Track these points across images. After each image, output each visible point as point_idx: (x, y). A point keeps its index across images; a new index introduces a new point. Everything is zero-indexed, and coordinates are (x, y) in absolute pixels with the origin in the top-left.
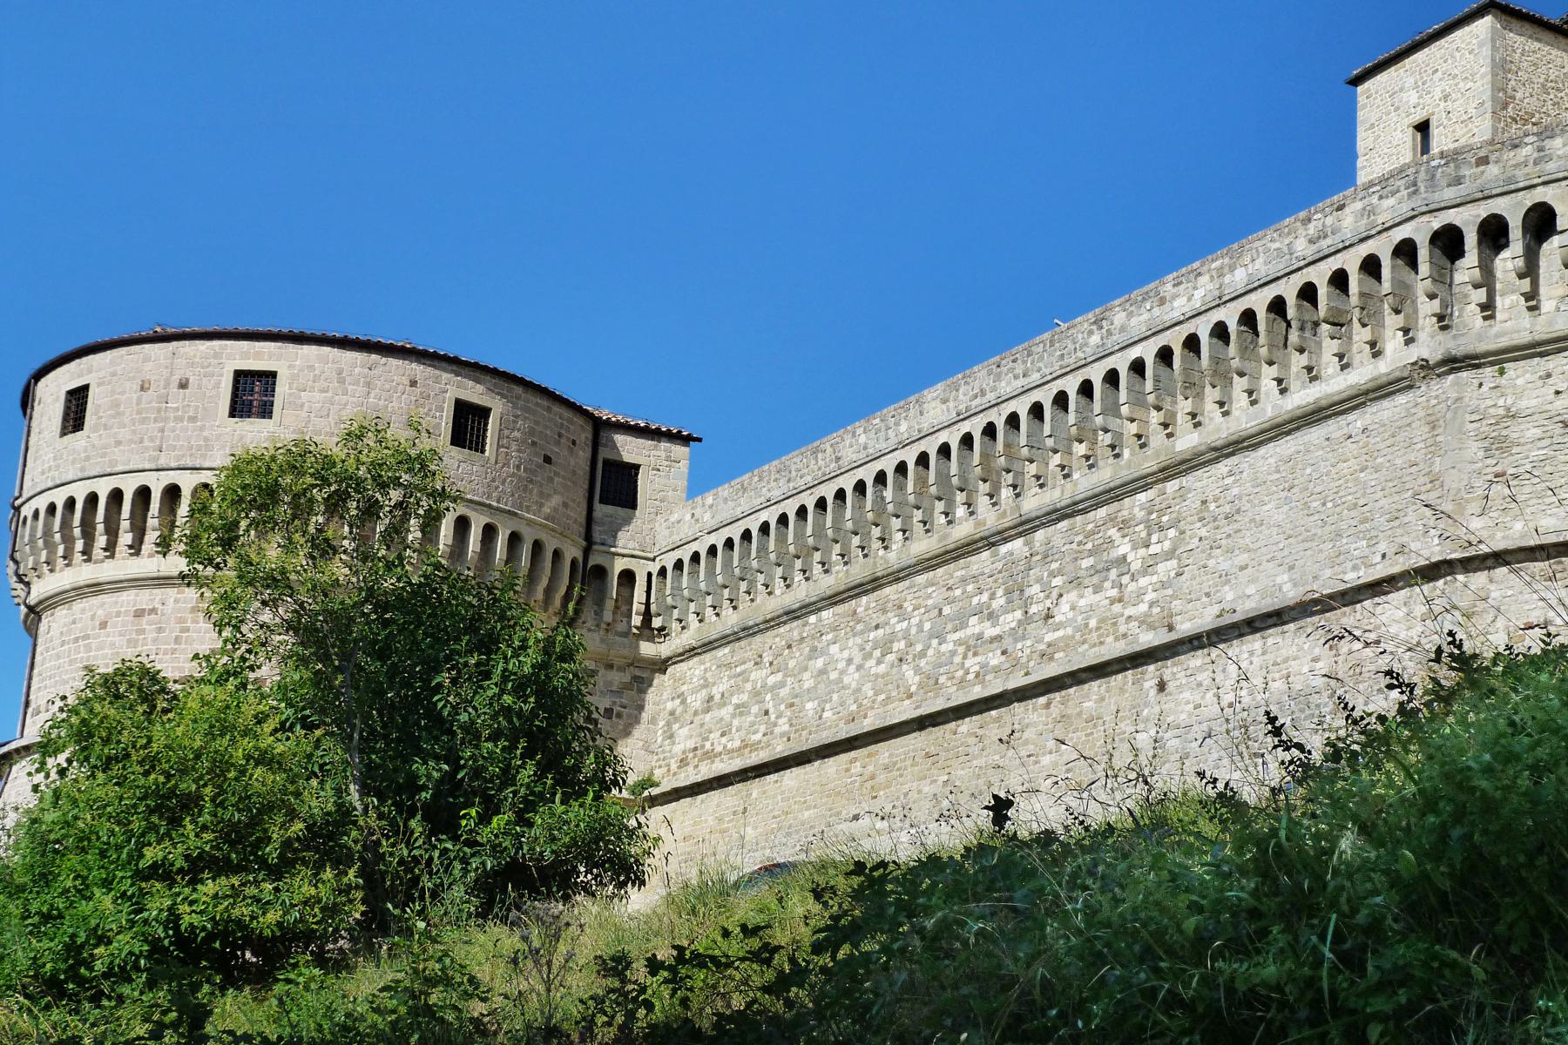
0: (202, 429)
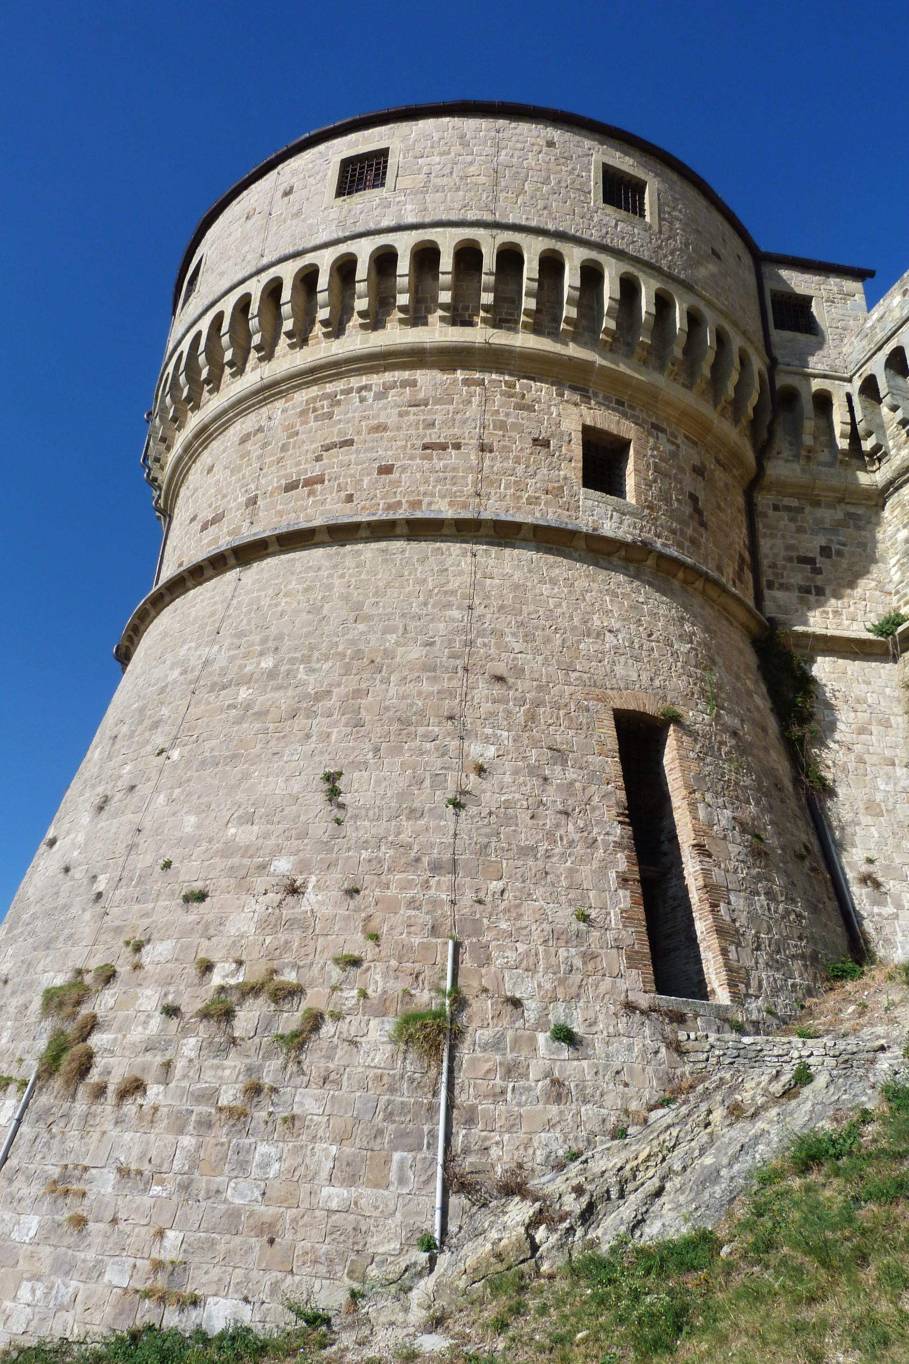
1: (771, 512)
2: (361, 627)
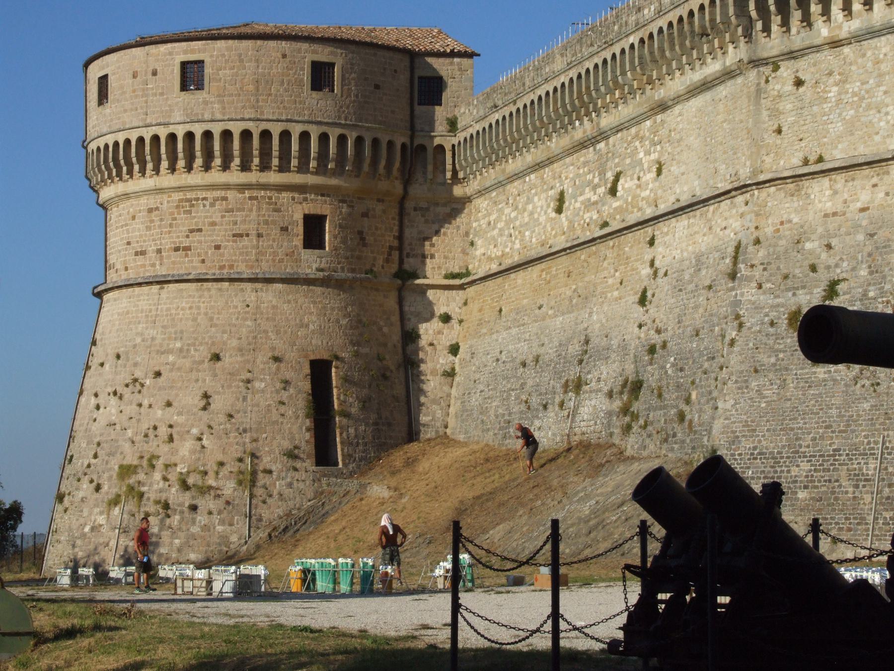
0: (167, 99)
1: (413, 213)
2: (213, 329)
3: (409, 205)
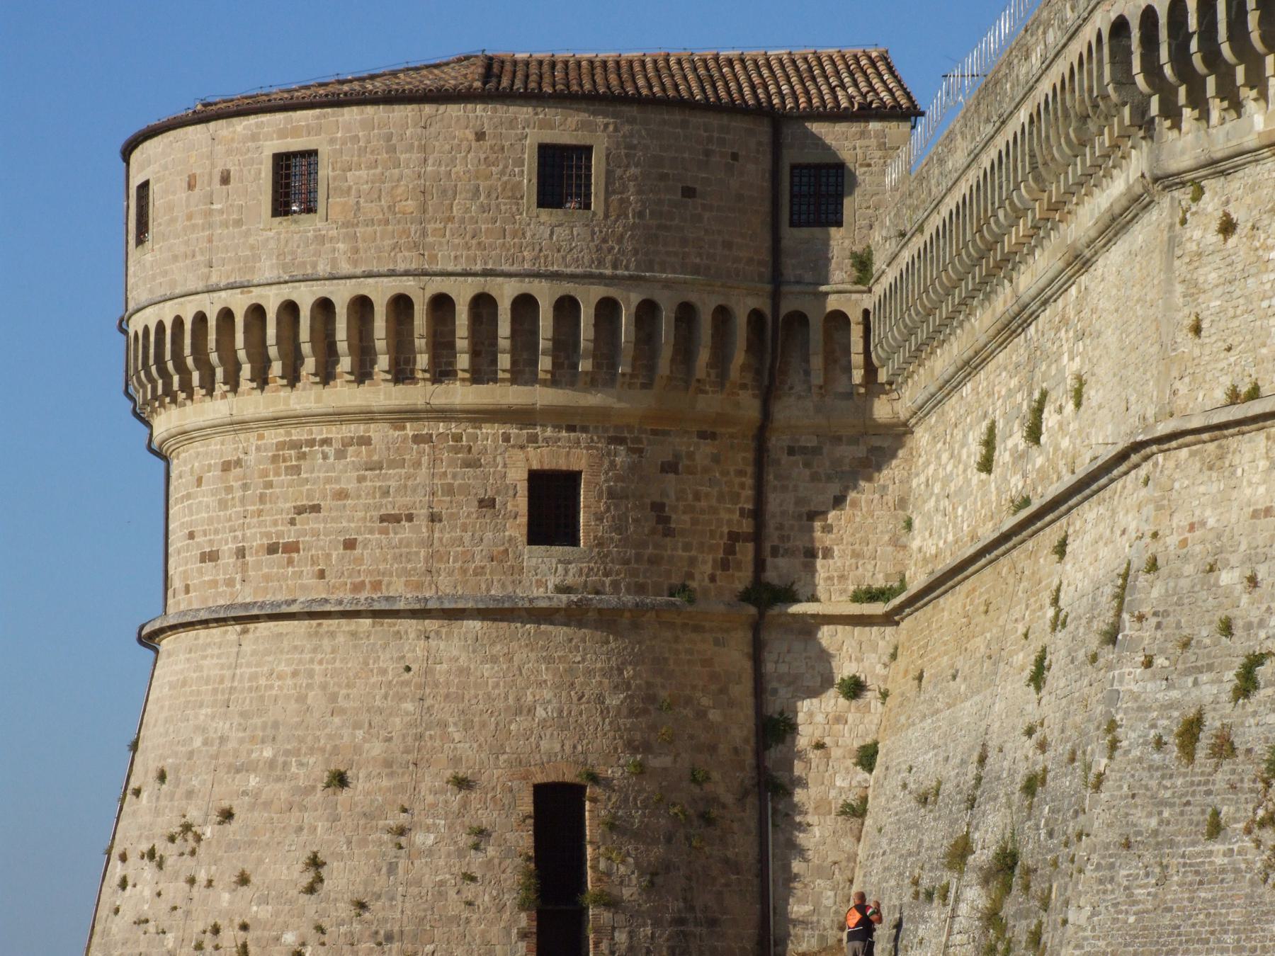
0: (247, 234)
1: (785, 458)
2: (337, 720)
3: (777, 442)
